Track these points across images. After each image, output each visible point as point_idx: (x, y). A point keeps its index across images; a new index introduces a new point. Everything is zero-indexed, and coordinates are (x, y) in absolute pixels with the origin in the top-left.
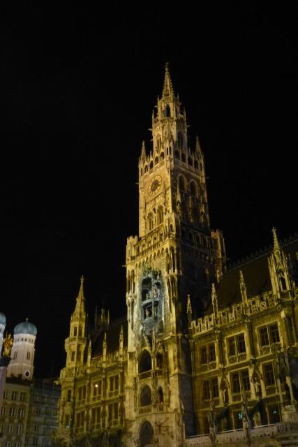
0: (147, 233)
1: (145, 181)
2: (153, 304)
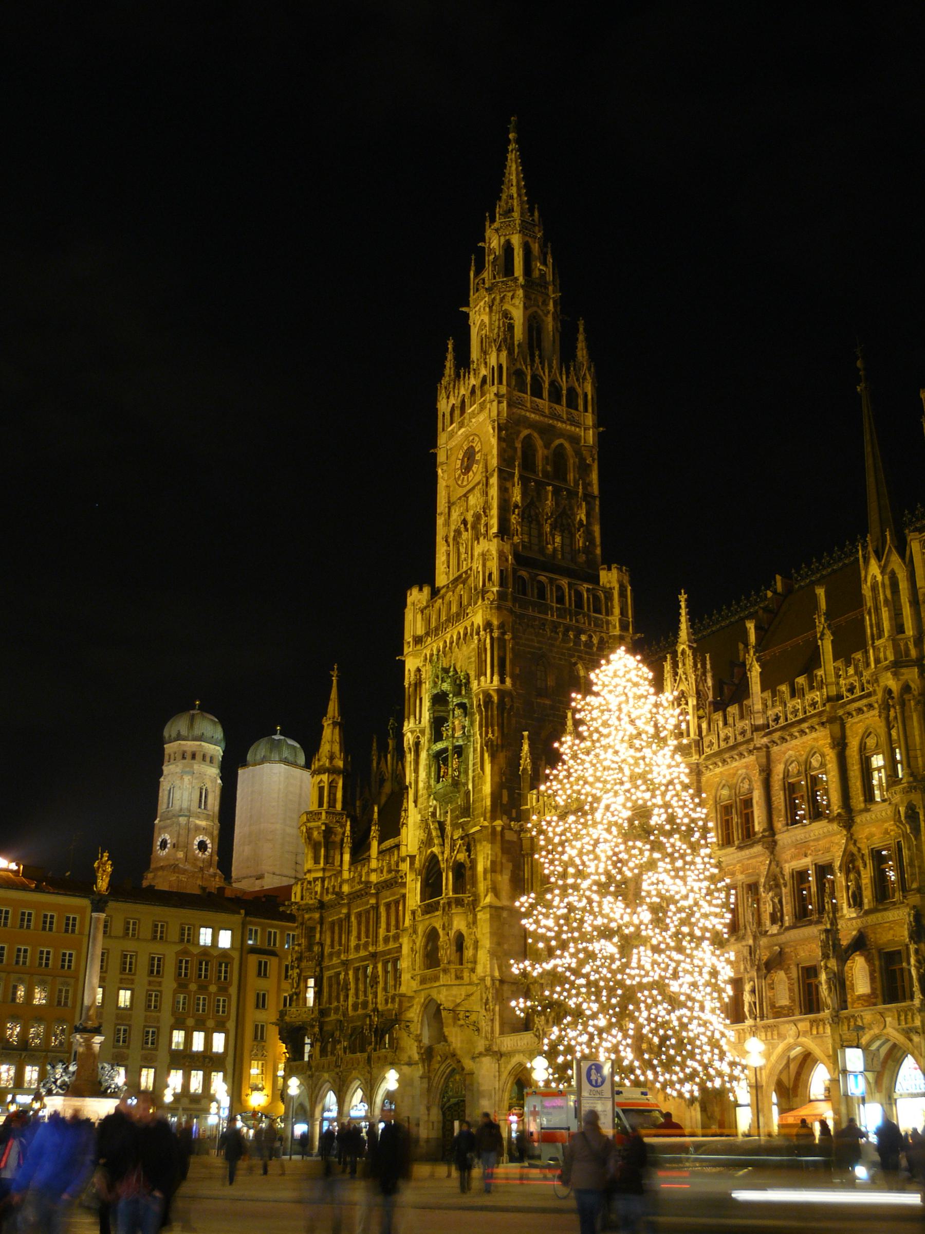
0: (451, 578)
1: (450, 442)
2: (450, 752)
